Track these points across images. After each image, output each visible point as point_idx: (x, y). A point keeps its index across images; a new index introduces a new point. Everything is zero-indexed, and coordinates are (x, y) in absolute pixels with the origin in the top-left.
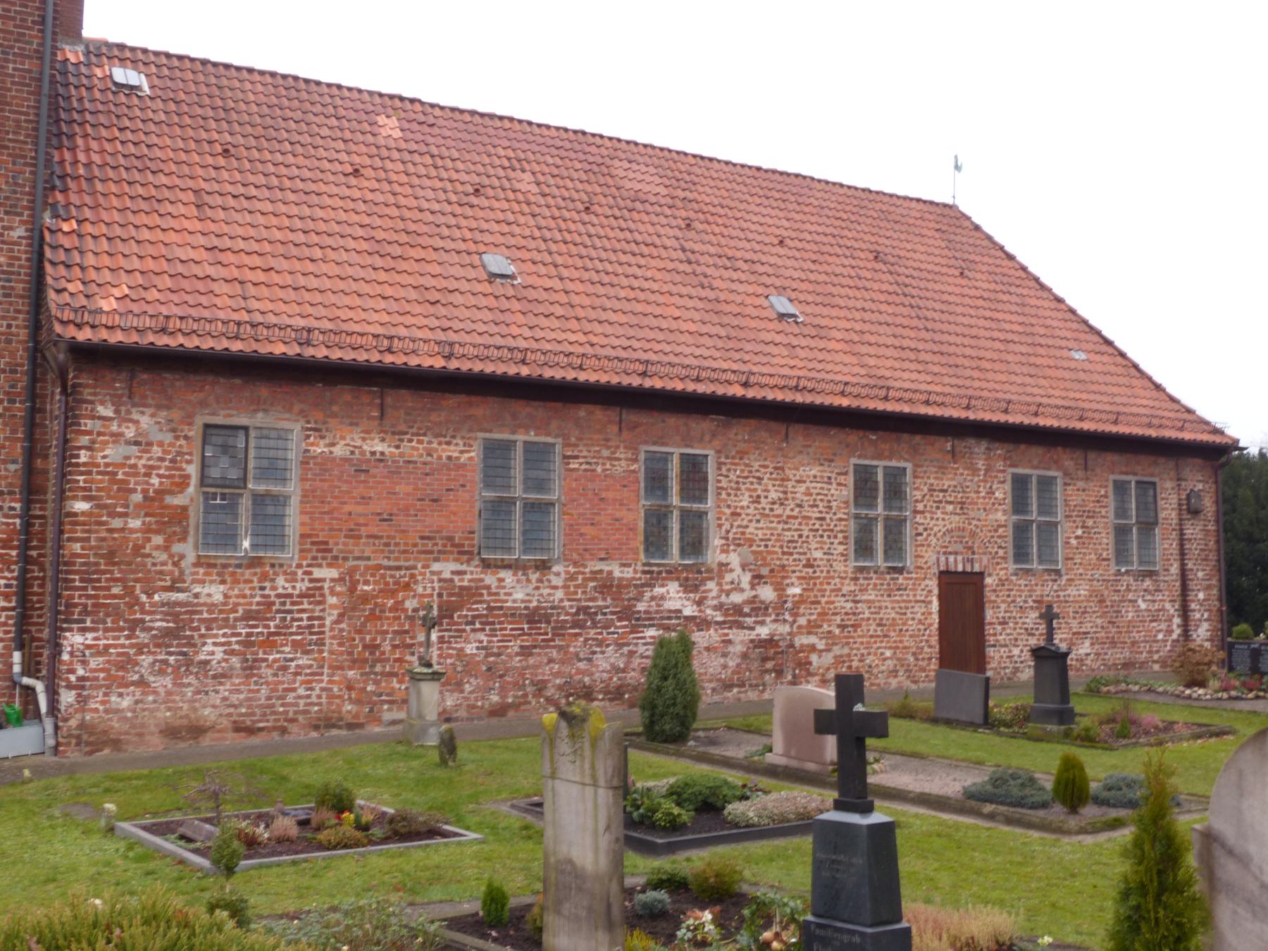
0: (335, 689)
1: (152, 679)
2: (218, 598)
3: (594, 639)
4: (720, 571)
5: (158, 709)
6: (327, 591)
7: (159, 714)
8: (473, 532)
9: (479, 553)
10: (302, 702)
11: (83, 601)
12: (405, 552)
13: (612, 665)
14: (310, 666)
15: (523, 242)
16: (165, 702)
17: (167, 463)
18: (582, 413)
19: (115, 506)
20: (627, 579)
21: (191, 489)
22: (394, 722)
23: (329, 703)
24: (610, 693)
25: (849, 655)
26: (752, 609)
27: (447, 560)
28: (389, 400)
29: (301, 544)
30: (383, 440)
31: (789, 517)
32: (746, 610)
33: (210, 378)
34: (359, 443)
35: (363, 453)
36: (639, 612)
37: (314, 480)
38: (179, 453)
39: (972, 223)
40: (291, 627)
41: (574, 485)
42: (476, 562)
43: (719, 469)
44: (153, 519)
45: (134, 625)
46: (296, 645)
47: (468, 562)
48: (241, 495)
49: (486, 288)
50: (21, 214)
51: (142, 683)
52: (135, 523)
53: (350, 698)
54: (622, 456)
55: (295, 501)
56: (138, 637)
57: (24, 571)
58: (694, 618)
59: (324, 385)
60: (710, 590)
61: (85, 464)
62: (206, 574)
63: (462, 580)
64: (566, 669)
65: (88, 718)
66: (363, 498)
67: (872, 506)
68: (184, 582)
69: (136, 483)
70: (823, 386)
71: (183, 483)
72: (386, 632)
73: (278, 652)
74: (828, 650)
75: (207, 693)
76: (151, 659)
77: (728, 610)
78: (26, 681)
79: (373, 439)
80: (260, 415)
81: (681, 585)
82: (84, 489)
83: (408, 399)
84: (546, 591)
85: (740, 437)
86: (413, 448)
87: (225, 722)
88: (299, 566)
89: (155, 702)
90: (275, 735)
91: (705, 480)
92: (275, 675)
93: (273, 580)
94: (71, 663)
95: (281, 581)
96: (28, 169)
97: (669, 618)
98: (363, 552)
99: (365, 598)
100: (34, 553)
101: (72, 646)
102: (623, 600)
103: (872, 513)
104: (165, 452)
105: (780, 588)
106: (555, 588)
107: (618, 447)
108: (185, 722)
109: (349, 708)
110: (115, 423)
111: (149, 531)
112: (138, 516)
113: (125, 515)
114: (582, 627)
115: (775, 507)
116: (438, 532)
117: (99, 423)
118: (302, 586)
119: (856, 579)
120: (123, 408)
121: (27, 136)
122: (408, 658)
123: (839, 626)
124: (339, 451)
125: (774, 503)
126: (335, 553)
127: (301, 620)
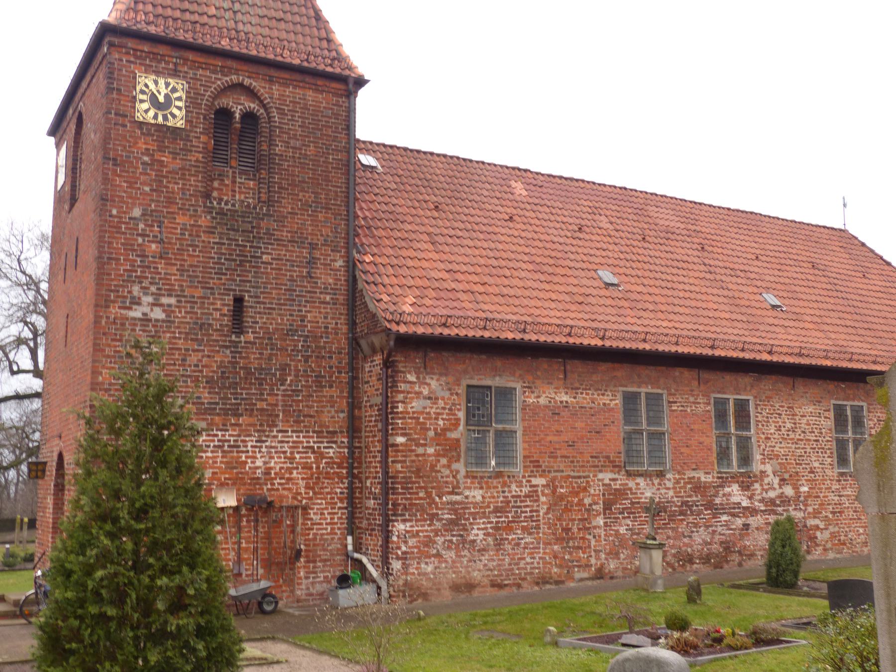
1: (444, 552)
4: (761, 476)
5: (448, 573)
6: (540, 493)
8: (620, 453)
10: (528, 567)
11: (404, 501)
12: (583, 466)
13: (703, 540)
14: (533, 543)
15: (616, 262)
18: (677, 374)
20: (709, 483)
21: (461, 428)
22: (582, 580)
23: (544, 568)
25: (838, 532)
26: (781, 502)
27: (606, 471)
28: (568, 367)
30: (567, 393)
31: (798, 440)
32: (778, 502)
33: (469, 355)
35: (556, 402)
38: (454, 404)
39: (859, 241)
42: (623, 472)
43: (756, 408)
44: (440, 448)
45: (433, 517)
46: (524, 529)
47: (619, 473)
48: (489, 431)
49: (603, 292)
50: (340, 252)
51: (438, 555)
52: (431, 450)
54: (701, 401)
55: (519, 434)
57: (351, 483)
58: (748, 508)
61: (401, 413)
62: (472, 483)
63: (615, 485)
64: (677, 543)
67: (845, 431)
69: (431, 424)
70: (812, 353)
71: (456, 425)
72: (575, 520)
74: (826, 529)
75: (475, 561)
76: (443, 539)
78: (356, 555)
80: (497, 378)
82: (402, 429)
83: (577, 367)
84: (663, 491)
86: (584, 398)
87: (486, 581)
88: (524, 477)
89: (446, 567)
90: (514, 589)
91: (749, 416)
92: (513, 549)
93: (509, 486)
95: (514, 487)
97: (734, 508)
99: (562, 497)
102: (707, 496)
103: (845, 436)
104: (445, 403)
105: (796, 488)
106: (668, 489)
107: (698, 395)
108: (463, 581)
113: (425, 445)
114: (685, 515)
115: (790, 433)
117: (408, 385)
118: (525, 490)
119: (839, 481)
120: (421, 376)
121: (342, 201)
122: (588, 537)
123: (832, 512)
124: (543, 401)
125: (789, 431)
127: (526, 512)
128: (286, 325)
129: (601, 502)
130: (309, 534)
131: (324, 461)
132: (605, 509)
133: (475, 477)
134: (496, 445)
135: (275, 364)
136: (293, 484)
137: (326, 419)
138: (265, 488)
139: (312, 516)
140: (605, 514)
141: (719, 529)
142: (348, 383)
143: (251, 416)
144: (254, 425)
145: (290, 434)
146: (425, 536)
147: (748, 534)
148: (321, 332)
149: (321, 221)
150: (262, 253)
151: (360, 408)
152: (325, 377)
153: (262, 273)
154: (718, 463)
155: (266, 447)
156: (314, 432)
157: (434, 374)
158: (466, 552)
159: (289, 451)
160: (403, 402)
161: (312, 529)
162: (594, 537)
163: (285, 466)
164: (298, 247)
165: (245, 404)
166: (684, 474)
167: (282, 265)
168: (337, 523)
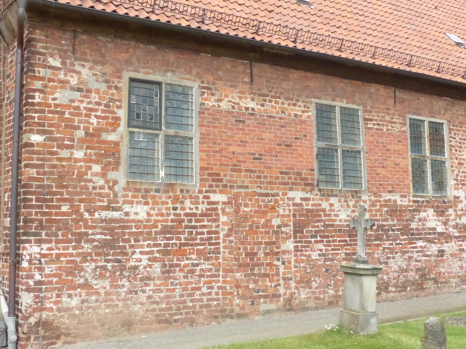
0: (228, 288)
1: (94, 282)
2: (143, 216)
3: (388, 248)
4: (455, 202)
5: (99, 307)
6: (220, 212)
7: (100, 311)
8: (313, 170)
9: (318, 185)
10: (205, 298)
12: (271, 183)
13: (399, 266)
14: (210, 270)
16: (105, 301)
17: (102, 107)
18: (373, 90)
20: (405, 206)
23: (224, 299)
24: (400, 287)
27: (297, 190)
28: (255, 71)
30: (253, 100)
33: (133, 43)
34: (237, 100)
35: (240, 108)
36: (413, 229)
37: (209, 126)
38: (111, 100)
40: (196, 239)
41: (371, 139)
43: (450, 133)
44: (93, 152)
45: (80, 237)
46: (199, 253)
47: (311, 191)
48: (157, 135)
51: (86, 286)
52: (79, 154)
53: (238, 294)
54: (397, 121)
55: (196, 142)
56: (83, 247)
59: (213, 56)
60: (451, 215)
61: (39, 104)
63: (307, 205)
65: (44, 316)
66: (242, 142)
68: (118, 203)
69: (79, 122)
73: (187, 259)
75: (136, 293)
76: (93, 265)
77: (460, 228)
79: (246, 98)
80: (169, 74)
81: (435, 211)
82: (39, 124)
85: (459, 113)
86: (272, 106)
87: (150, 316)
88: (200, 192)
89: (97, 301)
93: (182, 203)
94: (30, 269)
95: (188, 203)
97: (430, 234)
98: (244, 183)
99: (245, 218)
101: (30, 255)
104: (100, 97)
107: (394, 115)
109: (238, 302)
110: (62, 73)
112: (81, 148)
113: (71, 147)
114: (381, 240)
116: (292, 169)
117: (50, 71)
118: (203, 207)
120: (68, 61)
122: (276, 263)
124: (224, 105)
126: (224, 183)
127: (203, 233)
129: (292, 224)
132: (295, 232)
133: (136, 190)
140: (295, 237)
141: (415, 255)
146: (68, 262)
147: (443, 261)
154: (414, 186)
157: (85, 60)
162: (283, 263)
166: (380, 196)
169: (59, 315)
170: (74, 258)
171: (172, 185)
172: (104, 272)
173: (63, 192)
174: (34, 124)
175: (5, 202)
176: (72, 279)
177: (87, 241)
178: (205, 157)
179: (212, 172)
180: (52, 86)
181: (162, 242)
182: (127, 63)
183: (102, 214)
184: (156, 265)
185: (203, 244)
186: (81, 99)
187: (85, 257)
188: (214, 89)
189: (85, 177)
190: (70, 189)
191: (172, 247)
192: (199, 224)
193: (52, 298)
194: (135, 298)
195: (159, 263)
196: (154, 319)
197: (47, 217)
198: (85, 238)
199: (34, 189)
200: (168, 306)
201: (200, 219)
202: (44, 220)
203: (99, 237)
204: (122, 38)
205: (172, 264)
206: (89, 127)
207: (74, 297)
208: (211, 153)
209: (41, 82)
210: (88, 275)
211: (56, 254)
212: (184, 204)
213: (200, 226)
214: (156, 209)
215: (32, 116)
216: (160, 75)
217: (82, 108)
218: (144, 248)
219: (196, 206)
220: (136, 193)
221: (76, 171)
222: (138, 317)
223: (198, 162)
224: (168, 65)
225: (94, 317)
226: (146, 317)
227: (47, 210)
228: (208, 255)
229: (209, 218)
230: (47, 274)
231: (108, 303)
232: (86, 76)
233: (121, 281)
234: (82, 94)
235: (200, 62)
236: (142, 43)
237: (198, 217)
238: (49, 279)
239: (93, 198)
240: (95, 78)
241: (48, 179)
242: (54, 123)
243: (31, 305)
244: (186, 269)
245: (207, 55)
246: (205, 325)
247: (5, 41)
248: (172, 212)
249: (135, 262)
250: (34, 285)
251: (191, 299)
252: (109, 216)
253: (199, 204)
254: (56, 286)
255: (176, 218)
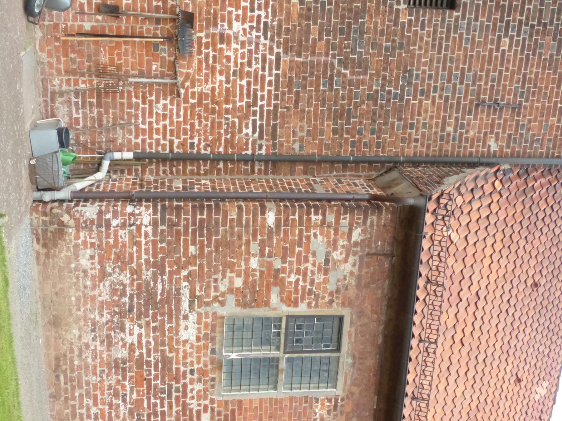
1: (107, 283)
5: (78, 290)
7: (73, 291)
10: (84, 411)
16: (84, 296)
19: (270, 246)
29: (232, 401)
33: (383, 318)
37: (290, 408)
40: (156, 398)
44: (257, 278)
45: (159, 267)
46: (139, 402)
48: (278, 349)
50: (508, 146)
51: (103, 275)
52: (254, 263)
55: (272, 394)
56: (148, 270)
57: (205, 159)
59: (375, 411)
61: (309, 220)
62: (206, 325)
65: (70, 230)
68: (199, 307)
73: (132, 388)
75: (93, 331)
78: (106, 164)
80: (350, 360)
82: (286, 220)
87: (65, 348)
88: (212, 401)
89: (85, 287)
92: (110, 387)
93: (199, 380)
94: (124, 214)
95: (198, 387)
96: (544, 151)
100: (221, 165)
101: (140, 214)
104: (319, 284)
110: (345, 243)
111: (247, 275)
112: (261, 265)
117: (346, 230)
118: (194, 405)
120: (358, 249)
127: (162, 406)
128: (418, 69)
130: (137, 97)
131: (236, 120)
133: (213, 329)
134: (258, 361)
135: (367, 53)
136: (207, 75)
137: (294, 123)
138: (203, 34)
139: (162, 102)
142: (339, 155)
143: (300, 16)
144: (288, 21)
145: (274, 72)
146: (131, 255)
148: (406, 119)
149: (547, 121)
150: (512, 37)
151: (305, 173)
152: (348, 123)
153: (487, 36)
155: (258, 37)
156: (276, 106)
157: (360, 267)
158: (106, 317)
159: (252, 70)
160: (323, 222)
161: (144, 103)
163: (232, 64)
164: (517, 88)
165: (316, 8)
167: (495, 66)
168: (151, 137)
169: (71, 246)
170: (135, 260)
171: (220, 368)
172: (119, 294)
173: (211, 248)
174: (286, 215)
175: (200, 180)
176: (111, 260)
177: (154, 274)
178: (254, 406)
179: (236, 414)
180: (330, 232)
181: (152, 359)
182: (360, 312)
183: (186, 290)
184: (125, 352)
185: (149, 407)
186: (317, 264)
187: (137, 272)
188: (335, 413)
189: (229, 270)
190: (214, 254)
191: (146, 370)
192: (174, 401)
193: (91, 238)
194: (86, 329)
195: (127, 355)
196: (61, 351)
197: (182, 230)
198: (159, 272)
199: (213, 216)
200: (76, 367)
201: (180, 401)
202: (179, 228)
203: (160, 287)
204: (389, 306)
205: (126, 370)
206: (285, 273)
207: (91, 261)
208: (258, 413)
209: (333, 221)
210: (115, 276)
211: (141, 242)
212: (197, 382)
213: (172, 402)
214: (191, 350)
215: (295, 212)
216: (348, 350)
217: (306, 265)
218: (145, 337)
219: (196, 397)
220: (210, 327)
221: (235, 261)
222: (64, 333)
223: (248, 398)
224: (360, 358)
225: (66, 284)
226: (64, 342)
227: (190, 231)
228: (135, 413)
229: (181, 413)
230: (118, 232)
231: (82, 299)
232: (343, 268)
233: (108, 313)
234: (322, 265)
235: (366, 396)
236: (385, 329)
237: (181, 400)
238: (112, 234)
239: (204, 279)
240: (342, 278)
241: (226, 230)
242: (288, 236)
243: (83, 216)
244: (120, 387)
245: (375, 404)
246: (51, 412)
247: (378, 177)
248: (188, 369)
249: (130, 328)
250: (105, 219)
251: (83, 395)
252: (183, 298)
253: (197, 400)
254: (104, 242)
255: (181, 373)
